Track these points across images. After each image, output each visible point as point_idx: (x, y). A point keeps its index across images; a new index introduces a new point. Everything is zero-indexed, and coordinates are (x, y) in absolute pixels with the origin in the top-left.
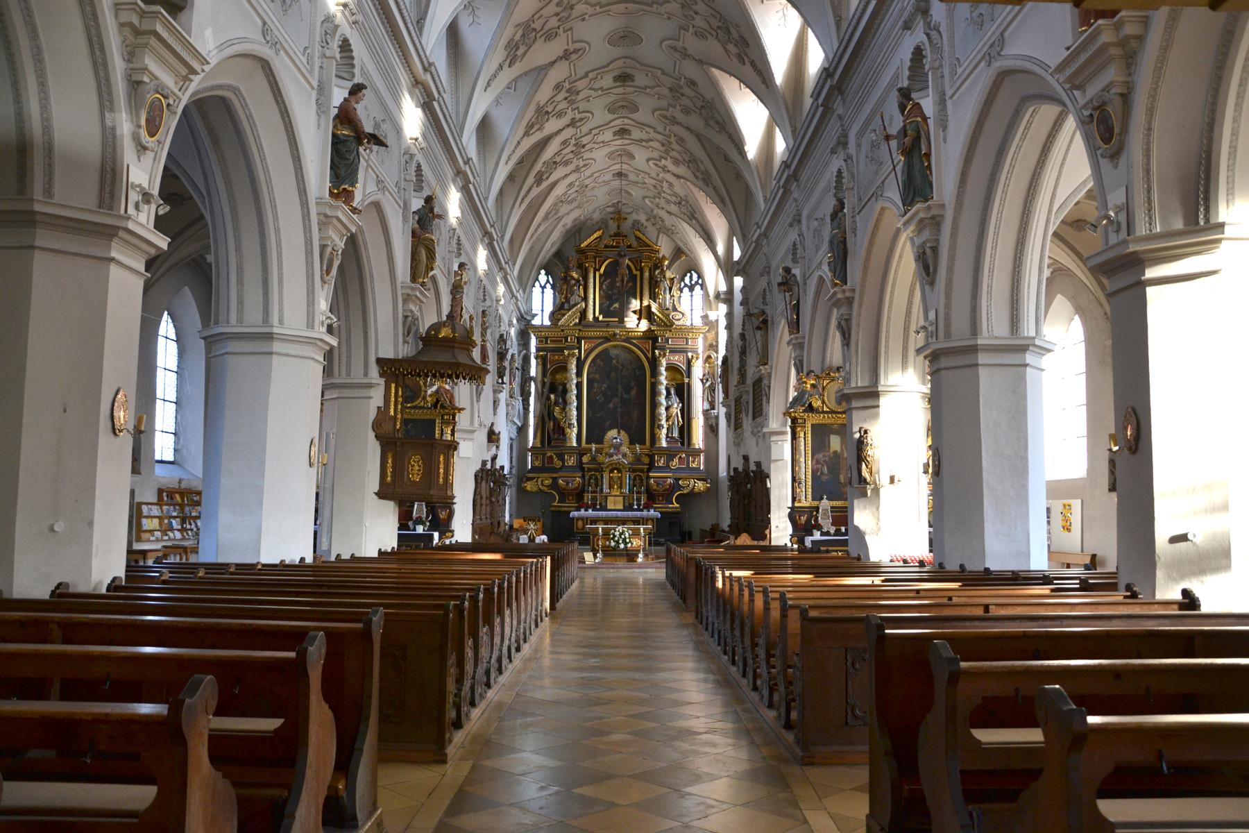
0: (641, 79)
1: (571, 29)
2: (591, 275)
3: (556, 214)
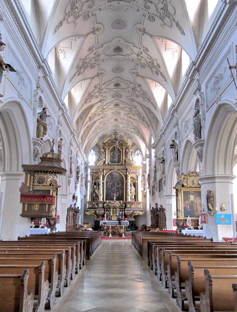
0: (123, 85)
1: (99, 64)
3: (96, 132)
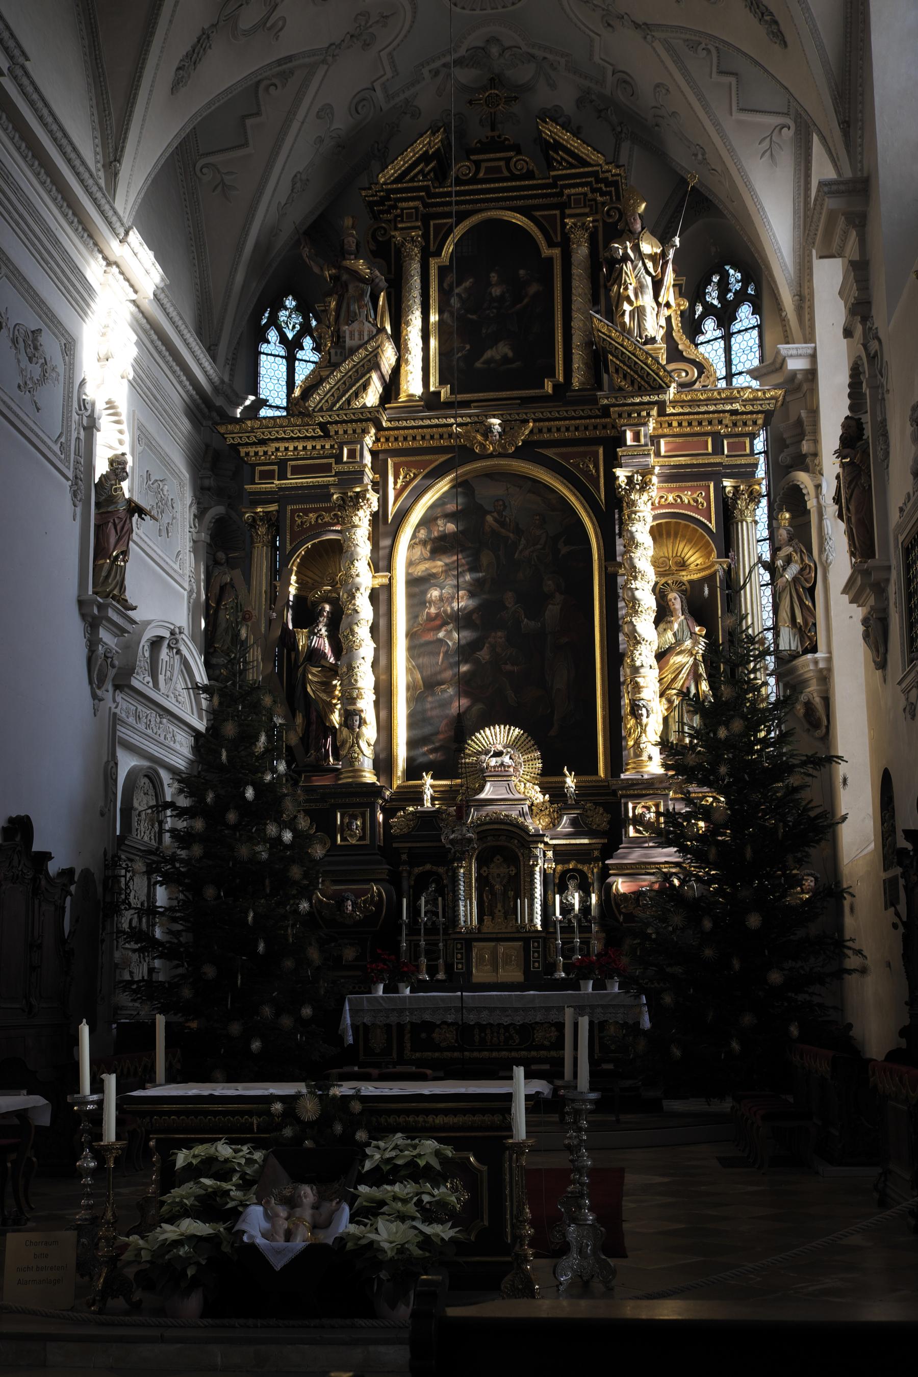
2: (415, 268)
